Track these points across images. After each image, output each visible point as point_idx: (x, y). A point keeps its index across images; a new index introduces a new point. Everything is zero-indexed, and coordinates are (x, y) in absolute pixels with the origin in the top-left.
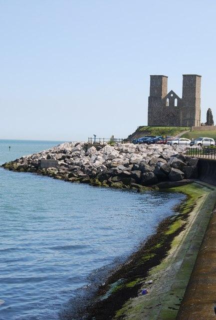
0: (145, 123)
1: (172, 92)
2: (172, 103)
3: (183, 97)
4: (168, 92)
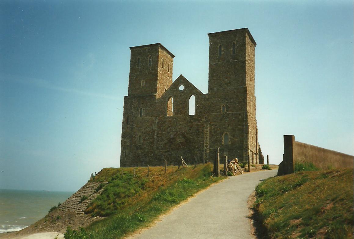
0: (114, 162)
2: (182, 106)
3: (210, 89)
4: (174, 78)
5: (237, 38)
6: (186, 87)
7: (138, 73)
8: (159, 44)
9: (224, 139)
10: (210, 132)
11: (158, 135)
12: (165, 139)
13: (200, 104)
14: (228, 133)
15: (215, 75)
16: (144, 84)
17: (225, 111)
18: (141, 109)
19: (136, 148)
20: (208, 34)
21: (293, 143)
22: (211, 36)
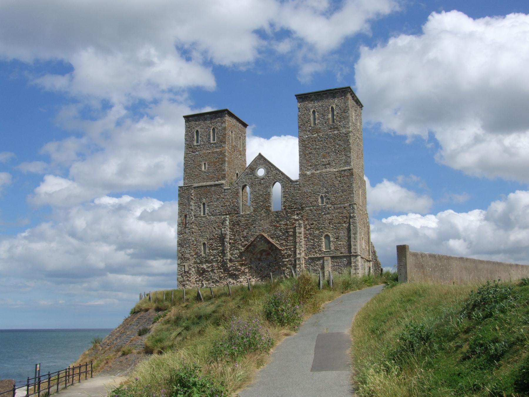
1: (261, 160)
2: (263, 199)
3: (302, 175)
6: (268, 172)
8: (227, 110)
9: (324, 243)
10: (305, 234)
11: (231, 241)
12: (240, 247)
14: (329, 234)
15: (307, 152)
16: (206, 169)
17: (325, 203)
18: (204, 204)
19: (199, 261)
20: (296, 96)
21: (408, 253)
22: (300, 98)
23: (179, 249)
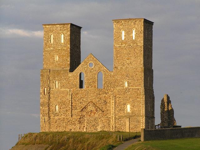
5: (136, 26)
7: (52, 49)
13: (107, 80)
15: (118, 55)
23: (41, 108)
